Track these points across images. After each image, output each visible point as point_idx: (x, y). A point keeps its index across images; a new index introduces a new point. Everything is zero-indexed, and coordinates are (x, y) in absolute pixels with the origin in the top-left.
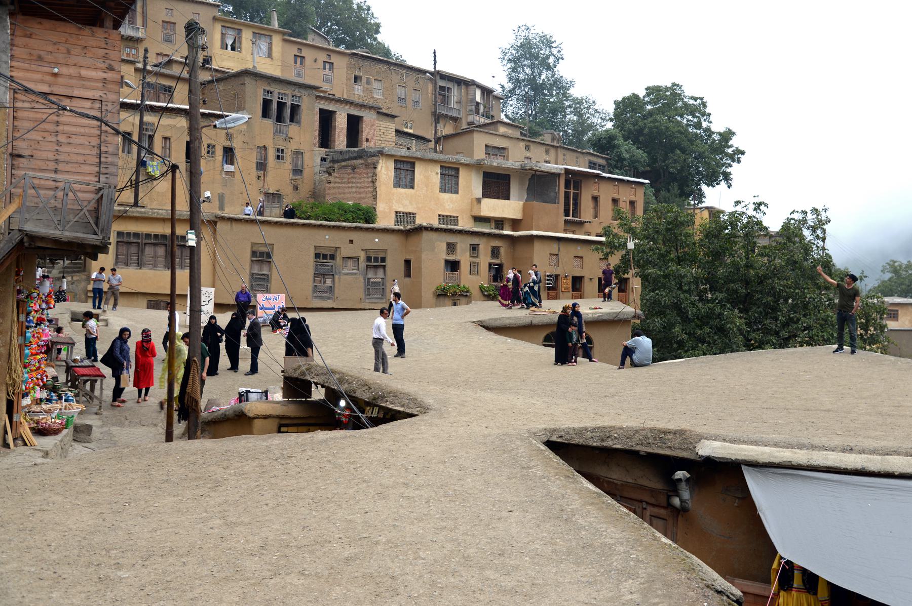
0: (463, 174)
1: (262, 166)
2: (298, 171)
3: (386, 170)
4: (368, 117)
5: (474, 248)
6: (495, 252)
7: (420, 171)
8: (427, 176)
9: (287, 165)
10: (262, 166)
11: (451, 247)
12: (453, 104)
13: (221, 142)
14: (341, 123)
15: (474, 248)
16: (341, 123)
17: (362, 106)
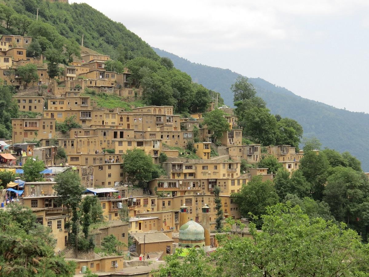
0: (132, 143)
1: (101, 144)
2: (109, 144)
3: (117, 143)
4: (124, 132)
5: (114, 156)
6: (118, 157)
7: (123, 143)
8: (125, 144)
9: (106, 142)
10: (101, 144)
11: (110, 157)
12: (162, 121)
13: (93, 141)
14: (119, 134)
15: (114, 156)
16: (119, 134)
17: (123, 130)
